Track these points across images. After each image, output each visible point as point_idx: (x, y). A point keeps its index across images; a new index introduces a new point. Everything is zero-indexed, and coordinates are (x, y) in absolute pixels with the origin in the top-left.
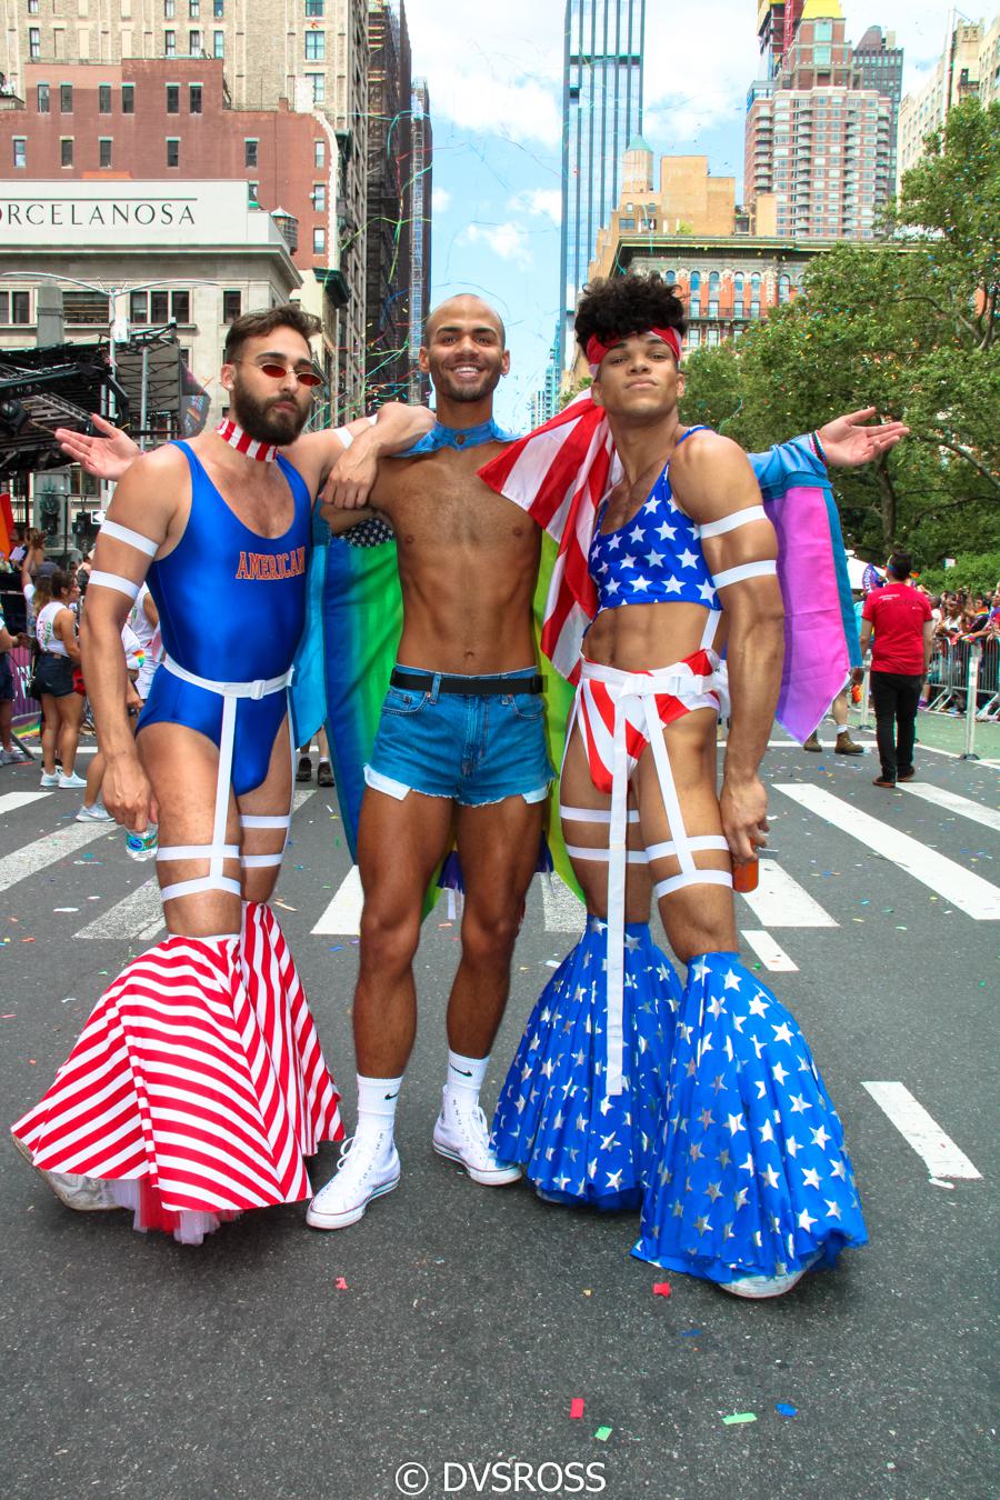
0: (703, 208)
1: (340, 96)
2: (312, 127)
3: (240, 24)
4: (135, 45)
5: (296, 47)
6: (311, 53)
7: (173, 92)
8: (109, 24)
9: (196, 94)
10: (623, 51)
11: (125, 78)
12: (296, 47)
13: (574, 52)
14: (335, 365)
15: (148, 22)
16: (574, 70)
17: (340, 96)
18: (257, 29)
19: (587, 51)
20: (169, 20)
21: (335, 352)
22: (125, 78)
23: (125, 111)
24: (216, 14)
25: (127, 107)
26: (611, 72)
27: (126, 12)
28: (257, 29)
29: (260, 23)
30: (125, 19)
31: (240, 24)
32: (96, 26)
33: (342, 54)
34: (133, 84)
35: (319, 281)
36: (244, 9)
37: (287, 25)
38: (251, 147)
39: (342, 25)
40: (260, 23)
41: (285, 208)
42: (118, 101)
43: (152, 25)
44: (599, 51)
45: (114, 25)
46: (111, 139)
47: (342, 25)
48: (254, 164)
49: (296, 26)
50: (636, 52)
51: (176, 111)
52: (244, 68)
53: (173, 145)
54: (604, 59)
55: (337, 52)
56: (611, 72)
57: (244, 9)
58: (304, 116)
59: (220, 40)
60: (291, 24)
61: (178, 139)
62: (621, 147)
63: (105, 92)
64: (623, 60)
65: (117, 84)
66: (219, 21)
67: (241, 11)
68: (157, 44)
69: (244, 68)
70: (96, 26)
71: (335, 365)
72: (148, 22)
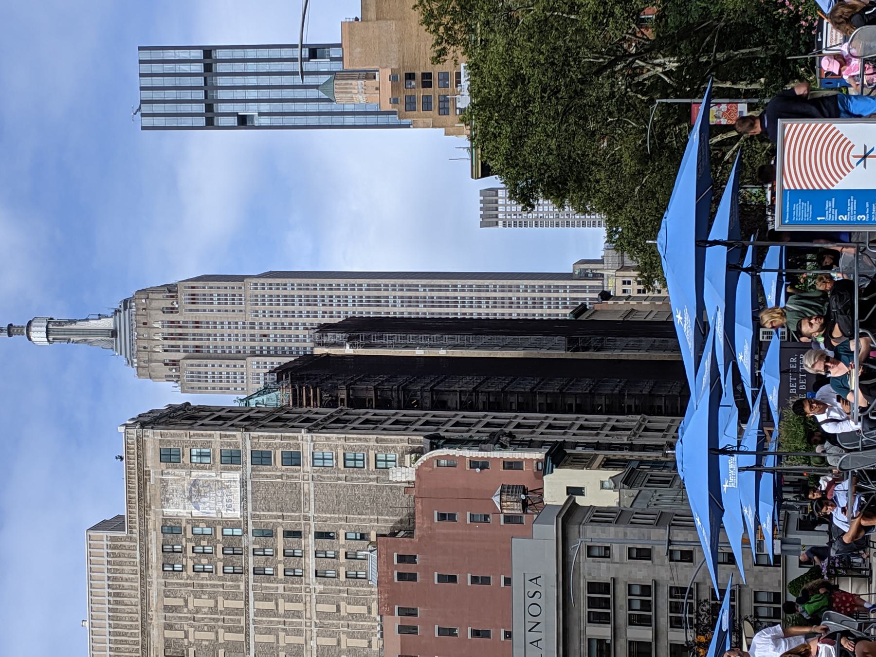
0: (392, 25)
1: (392, 441)
2: (425, 469)
3: (340, 519)
4: (357, 603)
5: (355, 476)
6: (359, 464)
7: (401, 576)
8: (342, 622)
9: (402, 559)
10: (199, 68)
11: (393, 614)
12: (355, 476)
13: (202, 121)
14: (618, 454)
15: (340, 591)
16: (222, 121)
17: (392, 441)
18: (343, 506)
19: (201, 108)
20: (338, 575)
21: (602, 454)
22: (393, 614)
23: (416, 615)
24: (332, 538)
25: (412, 613)
26: (221, 81)
27: (333, 608)
28: (343, 506)
29: (338, 503)
30: (338, 610)
31: (340, 519)
32: (344, 633)
33: (360, 439)
34: (396, 607)
35: (552, 472)
36: (329, 516)
37: (340, 482)
38: (442, 517)
39: (339, 439)
40: (338, 503)
41: (493, 494)
42: (410, 621)
43: (341, 588)
44: (200, 95)
45: (343, 618)
46: (437, 627)
47: (339, 439)
48: (454, 515)
49: (340, 475)
50: (199, 54)
51: (416, 574)
52: (372, 517)
53: (441, 578)
54: (208, 88)
55: (359, 443)
56: (221, 81)
57: (329, 516)
58: (418, 475)
59: (350, 536)
60: (339, 479)
61: (436, 574)
62: (333, 107)
63: (402, 629)
64: (208, 68)
65: (395, 621)
66: (338, 535)
67: (330, 518)
68: (355, 586)
69: (372, 517)
70: (344, 633)
71: (618, 454)
72: (340, 591)
